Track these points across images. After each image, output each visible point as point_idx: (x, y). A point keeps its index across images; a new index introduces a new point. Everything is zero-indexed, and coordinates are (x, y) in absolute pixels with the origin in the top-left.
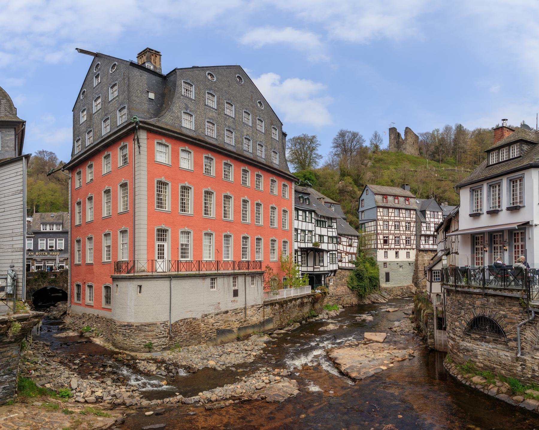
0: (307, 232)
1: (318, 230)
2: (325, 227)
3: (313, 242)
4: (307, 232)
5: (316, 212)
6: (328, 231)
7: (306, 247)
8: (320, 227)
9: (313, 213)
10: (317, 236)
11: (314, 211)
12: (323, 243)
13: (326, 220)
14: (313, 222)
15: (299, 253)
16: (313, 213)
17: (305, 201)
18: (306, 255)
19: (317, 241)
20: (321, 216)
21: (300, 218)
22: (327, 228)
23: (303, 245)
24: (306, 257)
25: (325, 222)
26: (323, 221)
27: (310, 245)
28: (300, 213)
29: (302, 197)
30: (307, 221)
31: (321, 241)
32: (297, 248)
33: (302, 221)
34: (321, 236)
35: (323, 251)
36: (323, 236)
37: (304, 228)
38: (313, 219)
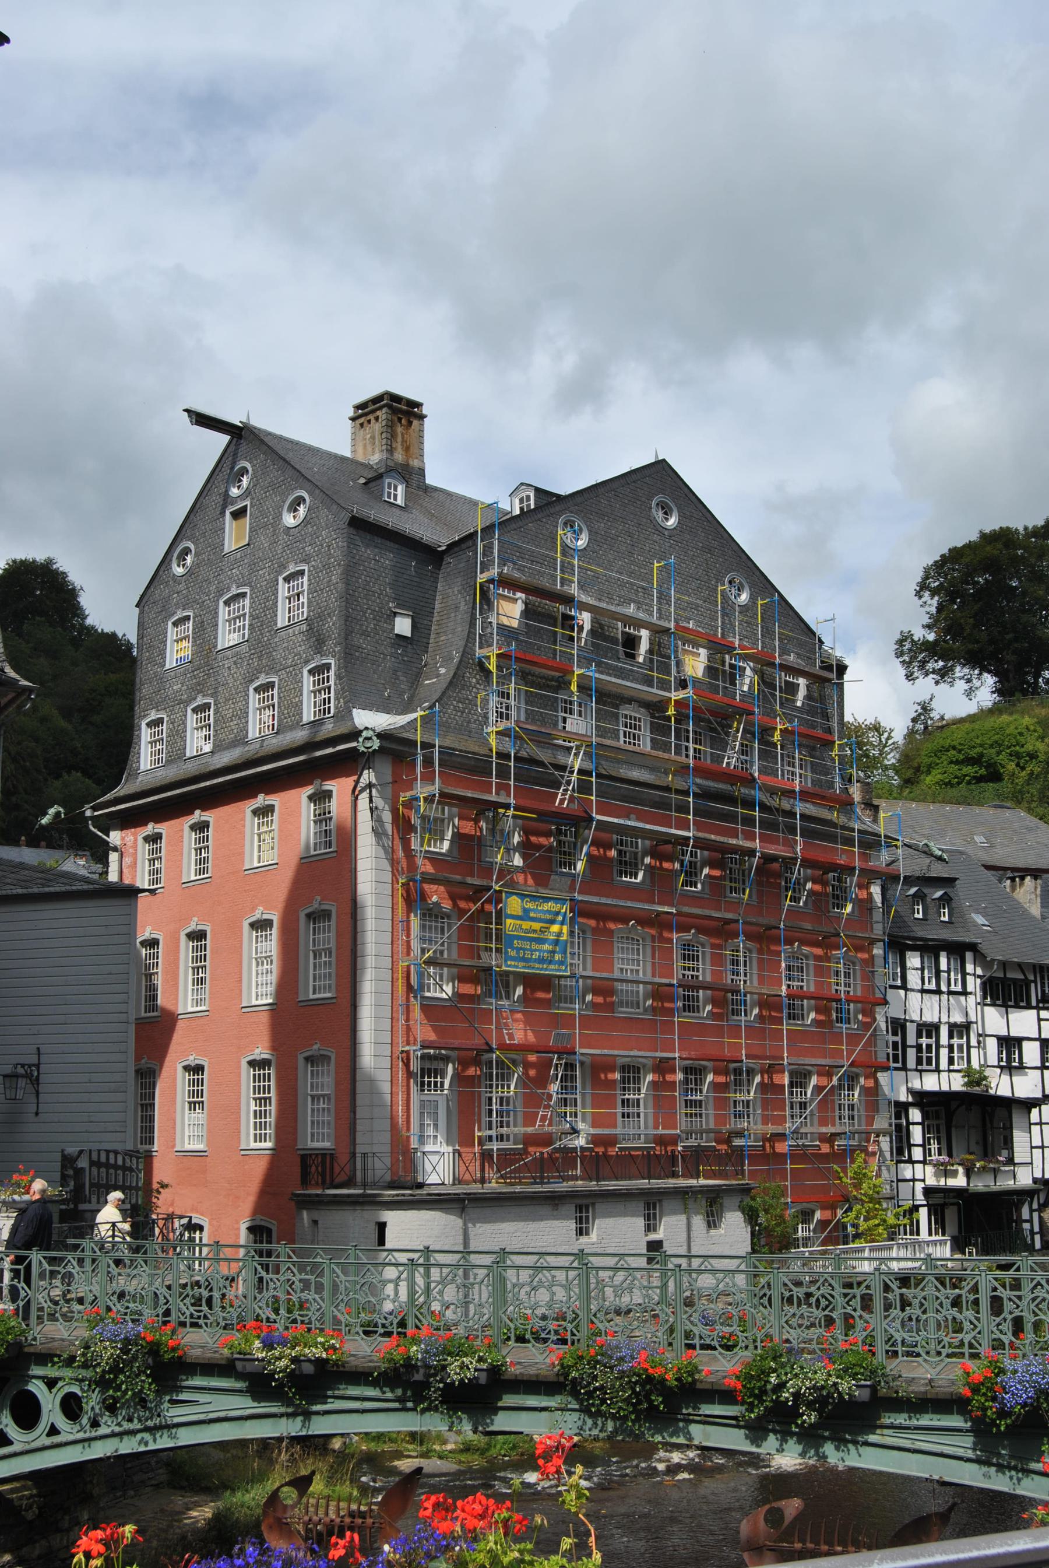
0: (944, 1031)
1: (994, 1021)
2: (1029, 1007)
3: (975, 1065)
4: (944, 1031)
5: (984, 948)
6: (1040, 1020)
7: (945, 1087)
8: (1007, 1007)
9: (969, 956)
10: (992, 1044)
11: (973, 947)
12: (1022, 1067)
13: (1032, 978)
14: (970, 988)
15: (915, 1115)
16: (969, 956)
17: (932, 911)
18: (942, 1122)
19: (993, 1060)
20: (1004, 965)
21: (914, 979)
22: (1038, 1008)
23: (930, 1083)
24: (943, 1129)
25: (1027, 983)
26: (1015, 980)
27: (957, 1083)
28: (914, 960)
29: (920, 897)
30: (944, 988)
31: (1009, 1059)
32: (903, 1097)
33: (923, 991)
34: (1010, 1044)
35: (1010, 1104)
36: (1019, 1041)
37: (930, 1017)
38: (970, 980)
